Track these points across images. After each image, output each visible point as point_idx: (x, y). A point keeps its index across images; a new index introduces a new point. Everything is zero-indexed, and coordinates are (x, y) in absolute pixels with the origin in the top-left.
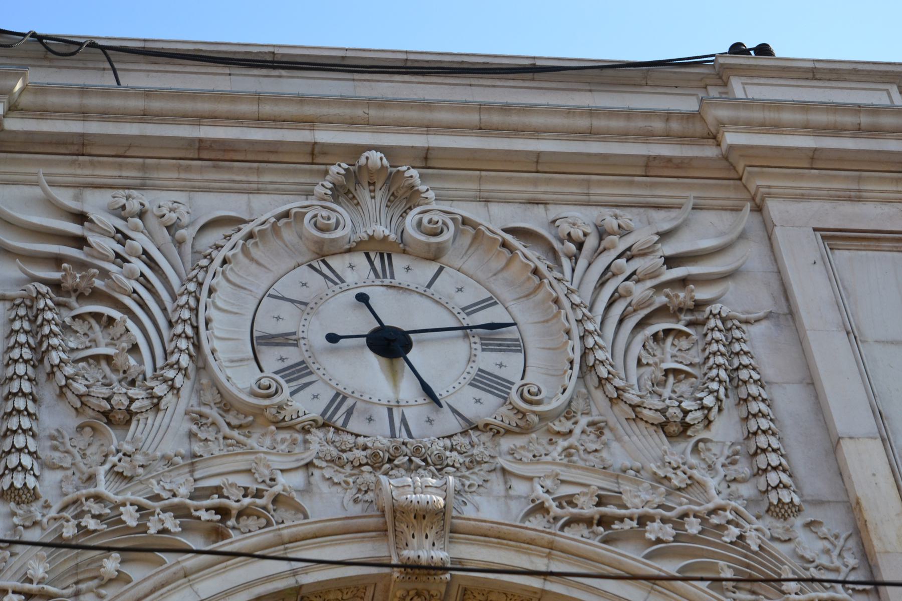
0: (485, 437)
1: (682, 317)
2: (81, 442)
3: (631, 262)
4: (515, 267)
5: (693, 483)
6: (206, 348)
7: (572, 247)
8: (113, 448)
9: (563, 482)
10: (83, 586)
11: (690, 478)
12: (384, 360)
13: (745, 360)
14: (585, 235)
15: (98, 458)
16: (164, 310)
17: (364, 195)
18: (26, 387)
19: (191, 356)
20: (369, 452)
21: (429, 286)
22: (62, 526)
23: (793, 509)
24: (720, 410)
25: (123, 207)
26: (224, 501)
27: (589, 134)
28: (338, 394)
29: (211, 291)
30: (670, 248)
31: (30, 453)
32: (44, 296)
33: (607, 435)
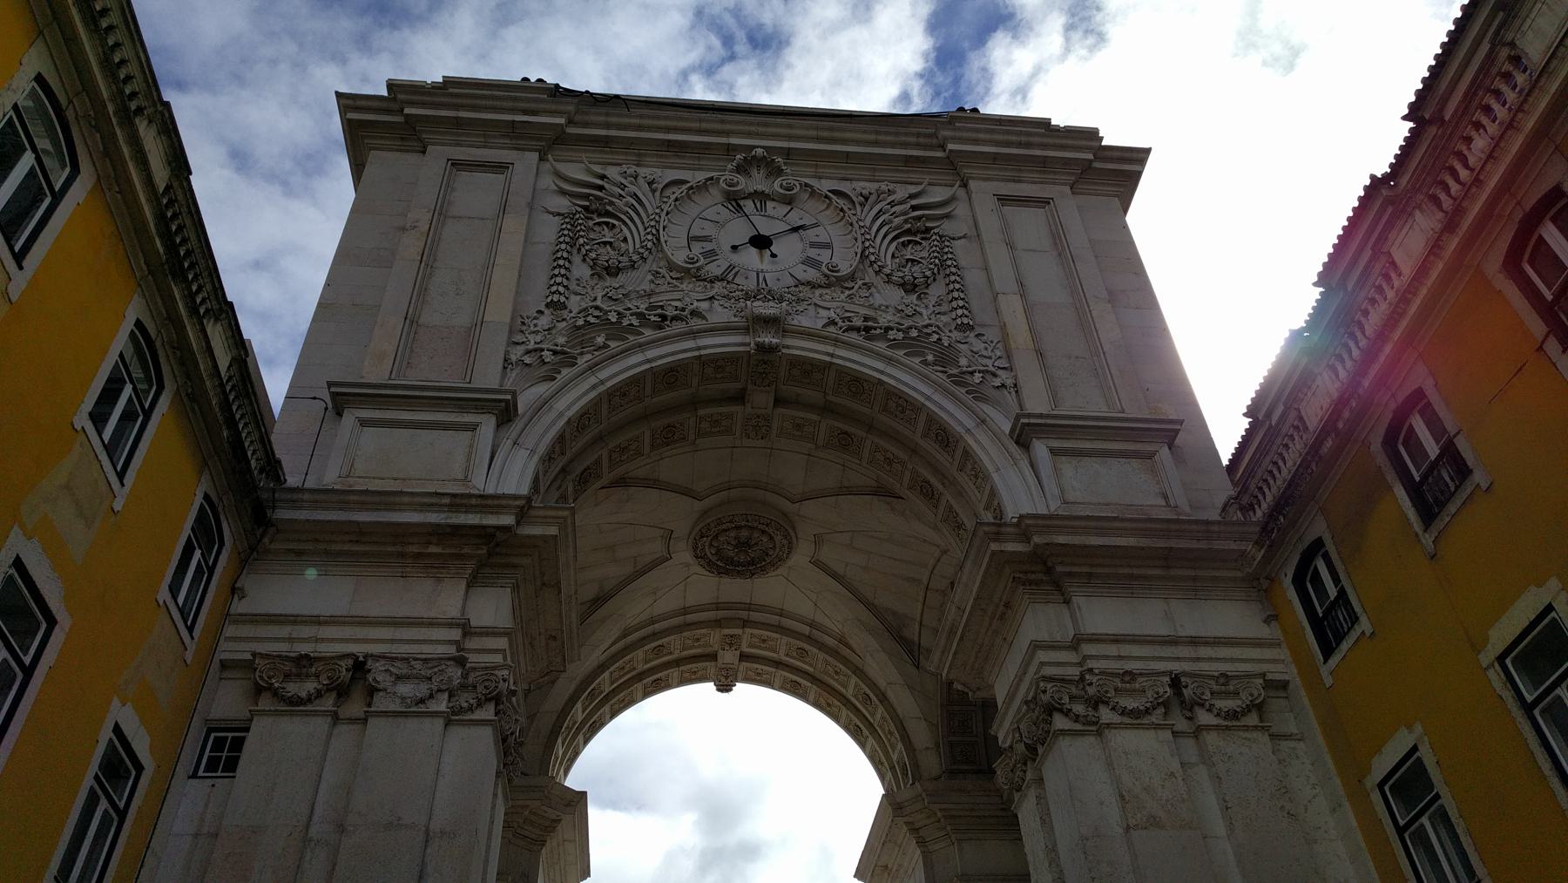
0: (808, 288)
2: (592, 283)
4: (832, 207)
6: (662, 240)
8: (608, 284)
9: (846, 311)
11: (915, 310)
12: (758, 251)
13: (950, 256)
16: (643, 223)
17: (754, 172)
18: (565, 255)
23: (972, 328)
24: (935, 280)
25: (626, 172)
29: (667, 214)
32: (579, 213)
33: (873, 289)
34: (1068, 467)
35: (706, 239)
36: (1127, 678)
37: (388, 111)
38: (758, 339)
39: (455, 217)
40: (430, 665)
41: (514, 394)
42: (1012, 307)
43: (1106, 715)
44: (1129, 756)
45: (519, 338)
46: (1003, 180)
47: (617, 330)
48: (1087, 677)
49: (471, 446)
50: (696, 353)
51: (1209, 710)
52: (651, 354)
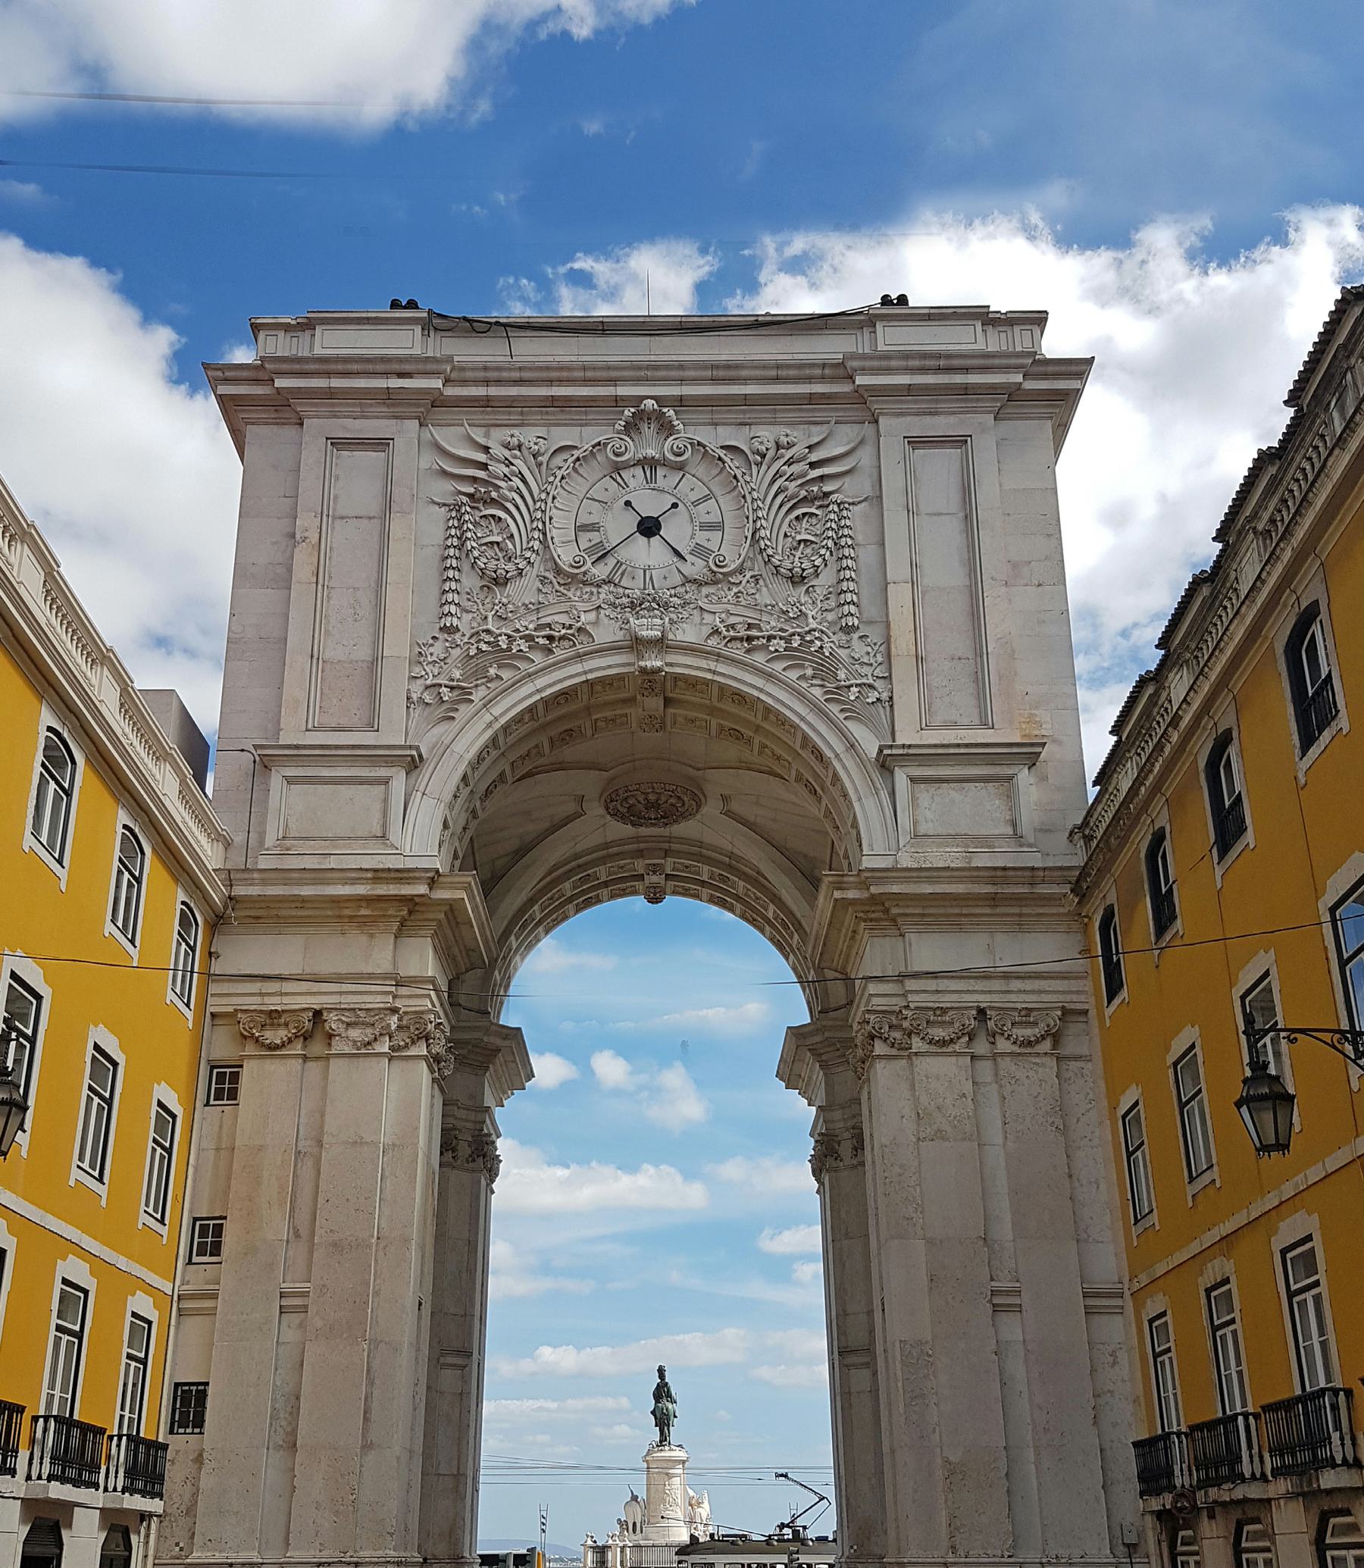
1: (816, 503)
2: (482, 596)
3: (792, 466)
4: (725, 473)
5: (802, 614)
7: (759, 458)
8: (497, 601)
9: (731, 614)
10: (479, 682)
11: (800, 611)
13: (846, 532)
14: (767, 449)
15: (490, 606)
16: (529, 509)
17: (644, 427)
18: (454, 563)
19: (540, 542)
20: (630, 599)
21: (675, 488)
22: (469, 648)
24: (826, 565)
26: (552, 632)
27: (777, 380)
28: (618, 562)
29: (554, 498)
30: (814, 457)
31: (455, 604)
33: (761, 582)
34: (925, 793)
35: (593, 527)
36: (938, 1012)
37: (256, 381)
38: (642, 664)
39: (342, 518)
40: (373, 1014)
41: (417, 748)
42: (900, 597)
43: (917, 1044)
44: (930, 1080)
45: (417, 671)
46: (917, 414)
47: (505, 657)
48: (904, 1012)
49: (386, 801)
50: (583, 678)
51: (1008, 1038)
52: (540, 682)
